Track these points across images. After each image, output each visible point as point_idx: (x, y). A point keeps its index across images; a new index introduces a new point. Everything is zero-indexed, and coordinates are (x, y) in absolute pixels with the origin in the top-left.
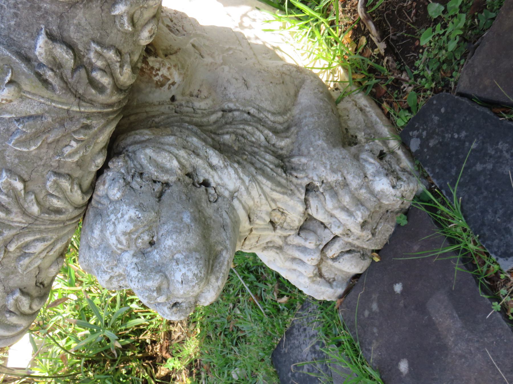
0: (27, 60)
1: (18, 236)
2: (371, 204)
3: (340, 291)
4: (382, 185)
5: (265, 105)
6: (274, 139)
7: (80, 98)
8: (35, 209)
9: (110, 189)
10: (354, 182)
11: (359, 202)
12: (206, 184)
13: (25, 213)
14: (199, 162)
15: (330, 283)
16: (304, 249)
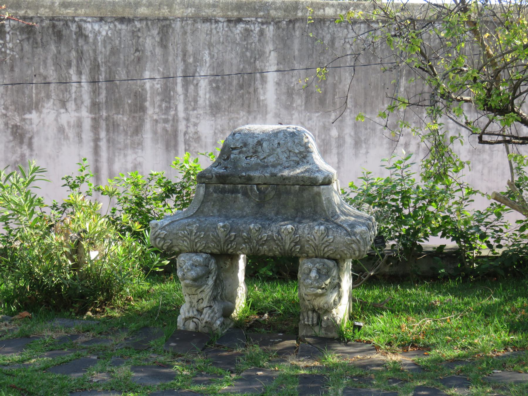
0: (230, 232)
1: (188, 239)
2: (213, 321)
3: (182, 329)
4: (218, 322)
5: (226, 292)
6: (219, 295)
7: (224, 243)
8: (196, 241)
9: (204, 256)
10: (217, 315)
11: (212, 318)
12: (208, 277)
13: (195, 239)
14: (213, 274)
15: (184, 325)
16: (193, 312)
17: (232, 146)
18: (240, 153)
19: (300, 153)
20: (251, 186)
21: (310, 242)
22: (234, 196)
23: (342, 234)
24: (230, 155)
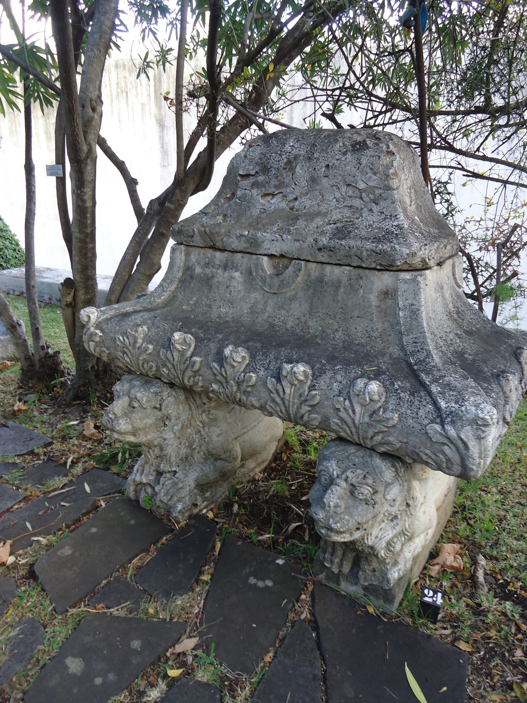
17: (241, 172)
18: (253, 185)
19: (370, 190)
20: (258, 258)
21: (340, 414)
22: (226, 274)
23: (421, 413)
24: (236, 190)
